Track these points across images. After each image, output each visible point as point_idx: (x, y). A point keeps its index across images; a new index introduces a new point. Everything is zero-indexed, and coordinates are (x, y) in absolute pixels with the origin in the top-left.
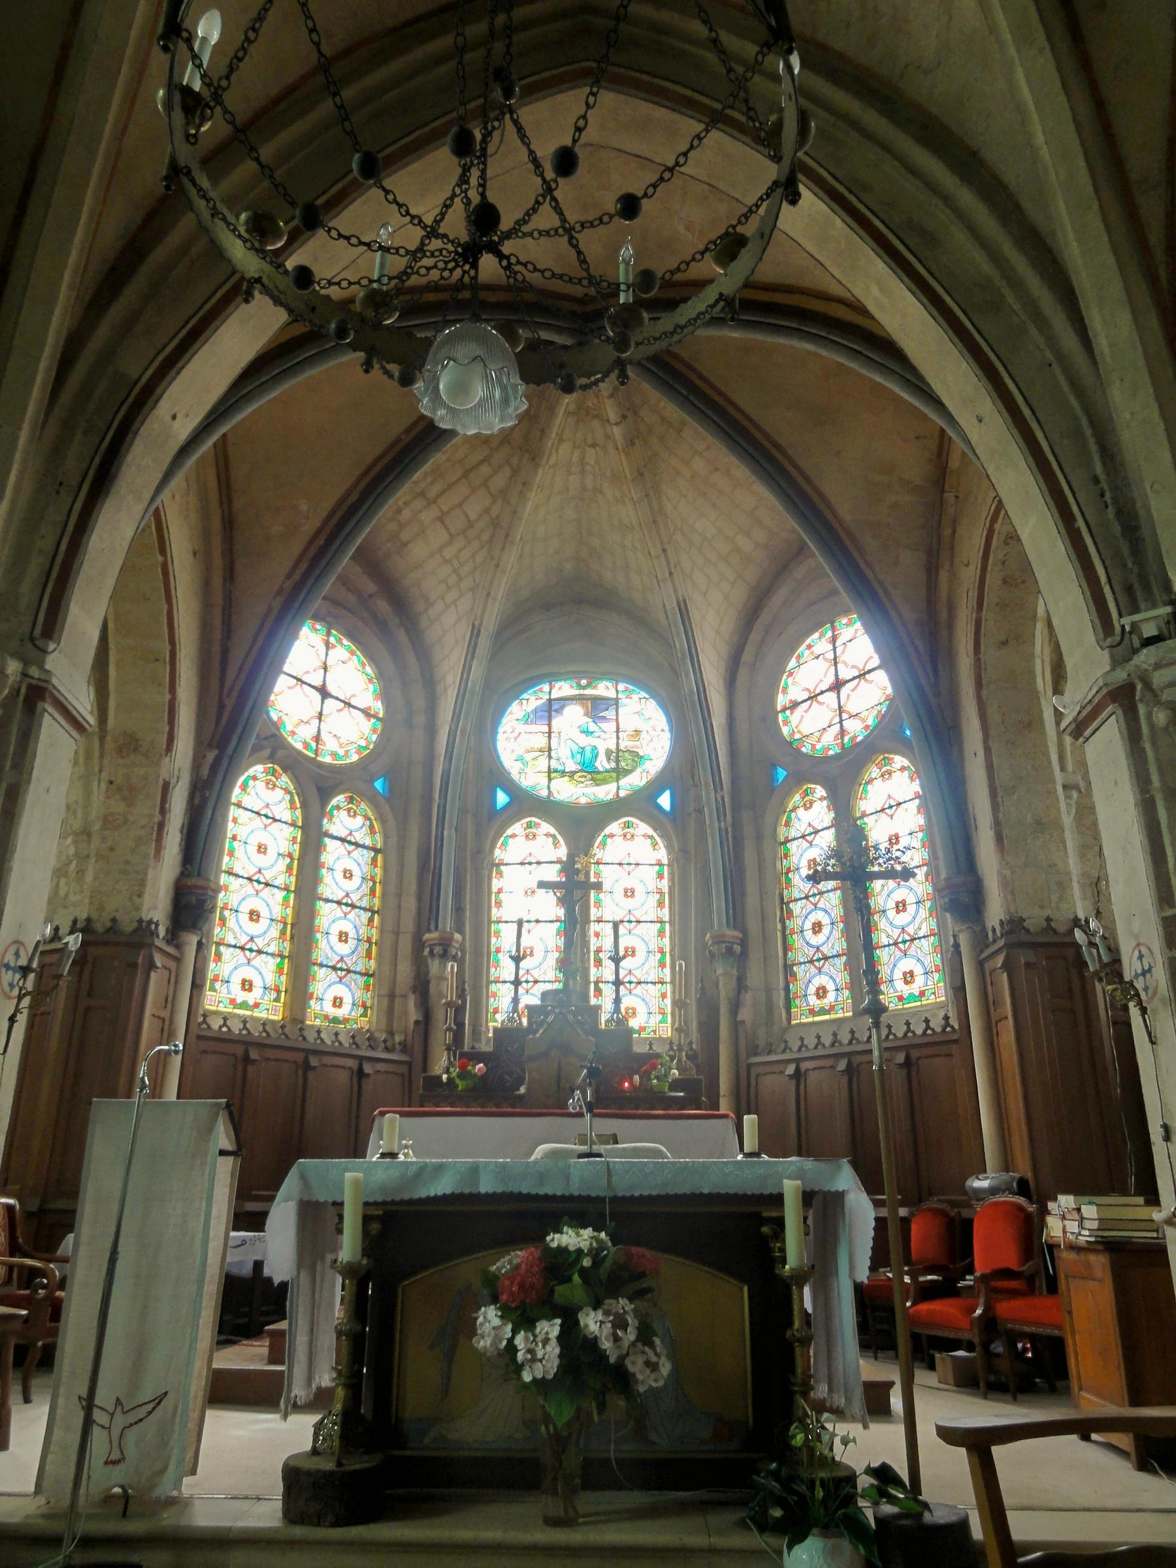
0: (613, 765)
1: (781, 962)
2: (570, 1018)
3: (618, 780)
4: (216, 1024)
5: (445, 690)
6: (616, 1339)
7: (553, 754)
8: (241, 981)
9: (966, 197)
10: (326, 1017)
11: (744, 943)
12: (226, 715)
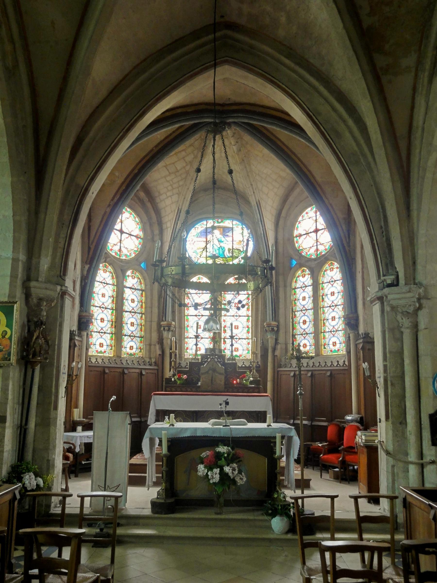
0: (231, 255)
1: (291, 333)
2: (216, 360)
4: (93, 360)
5: (167, 228)
6: (233, 473)
7: (208, 250)
8: (99, 344)
9: (350, 122)
10: (128, 354)
11: (278, 327)
12: (91, 253)
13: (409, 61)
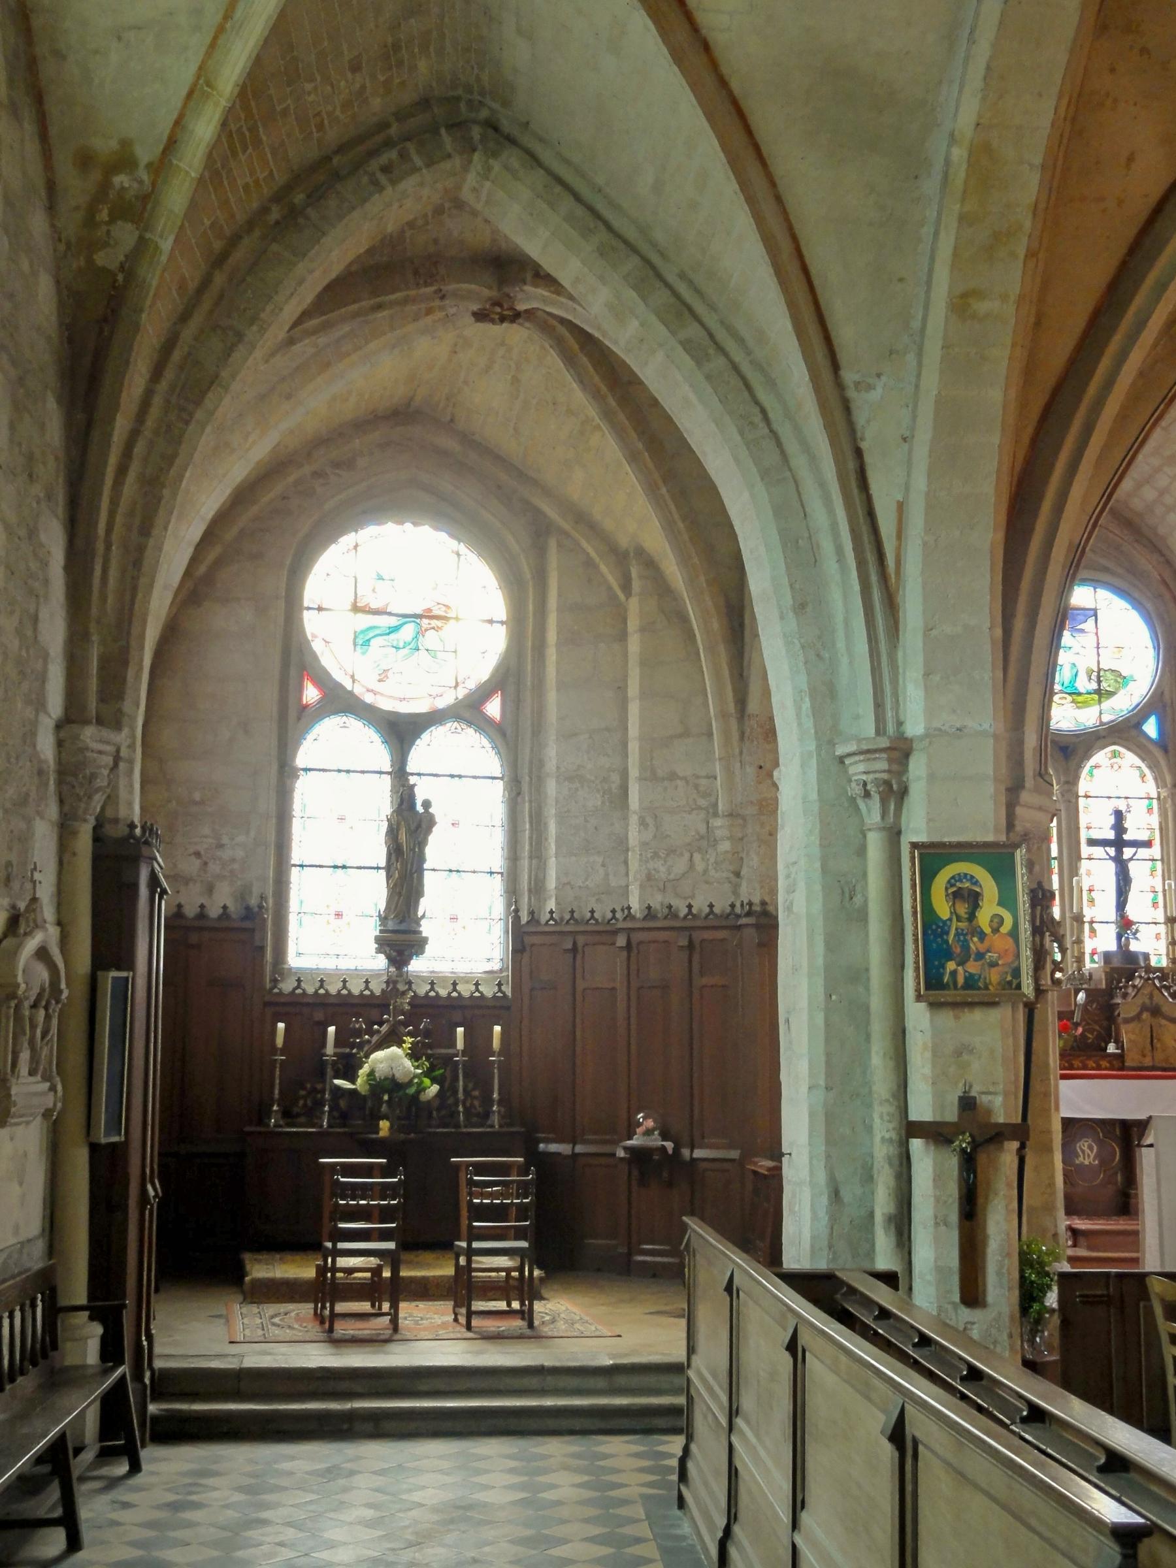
0: (1094, 686)
3: (1100, 702)
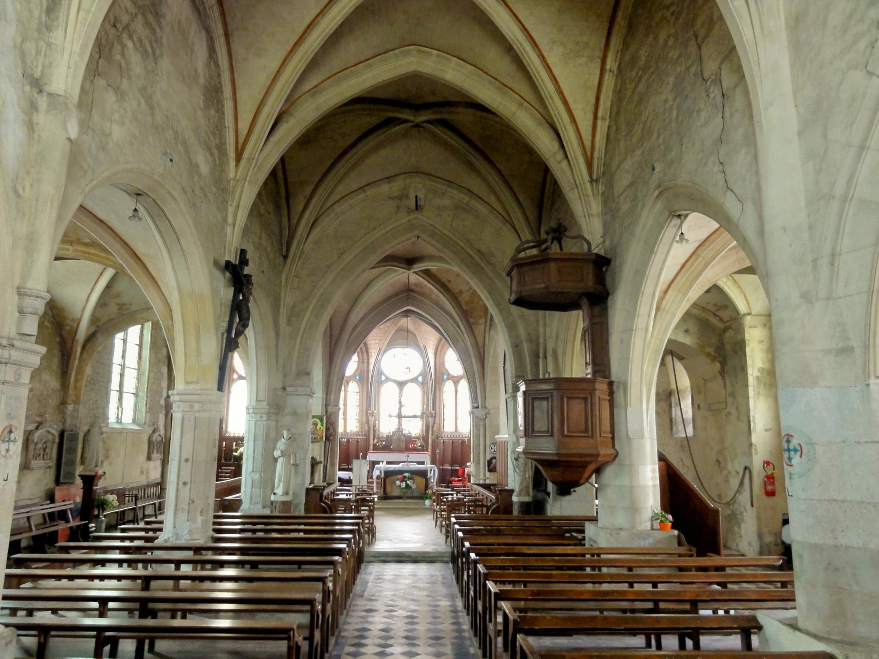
13: (482, 321)
